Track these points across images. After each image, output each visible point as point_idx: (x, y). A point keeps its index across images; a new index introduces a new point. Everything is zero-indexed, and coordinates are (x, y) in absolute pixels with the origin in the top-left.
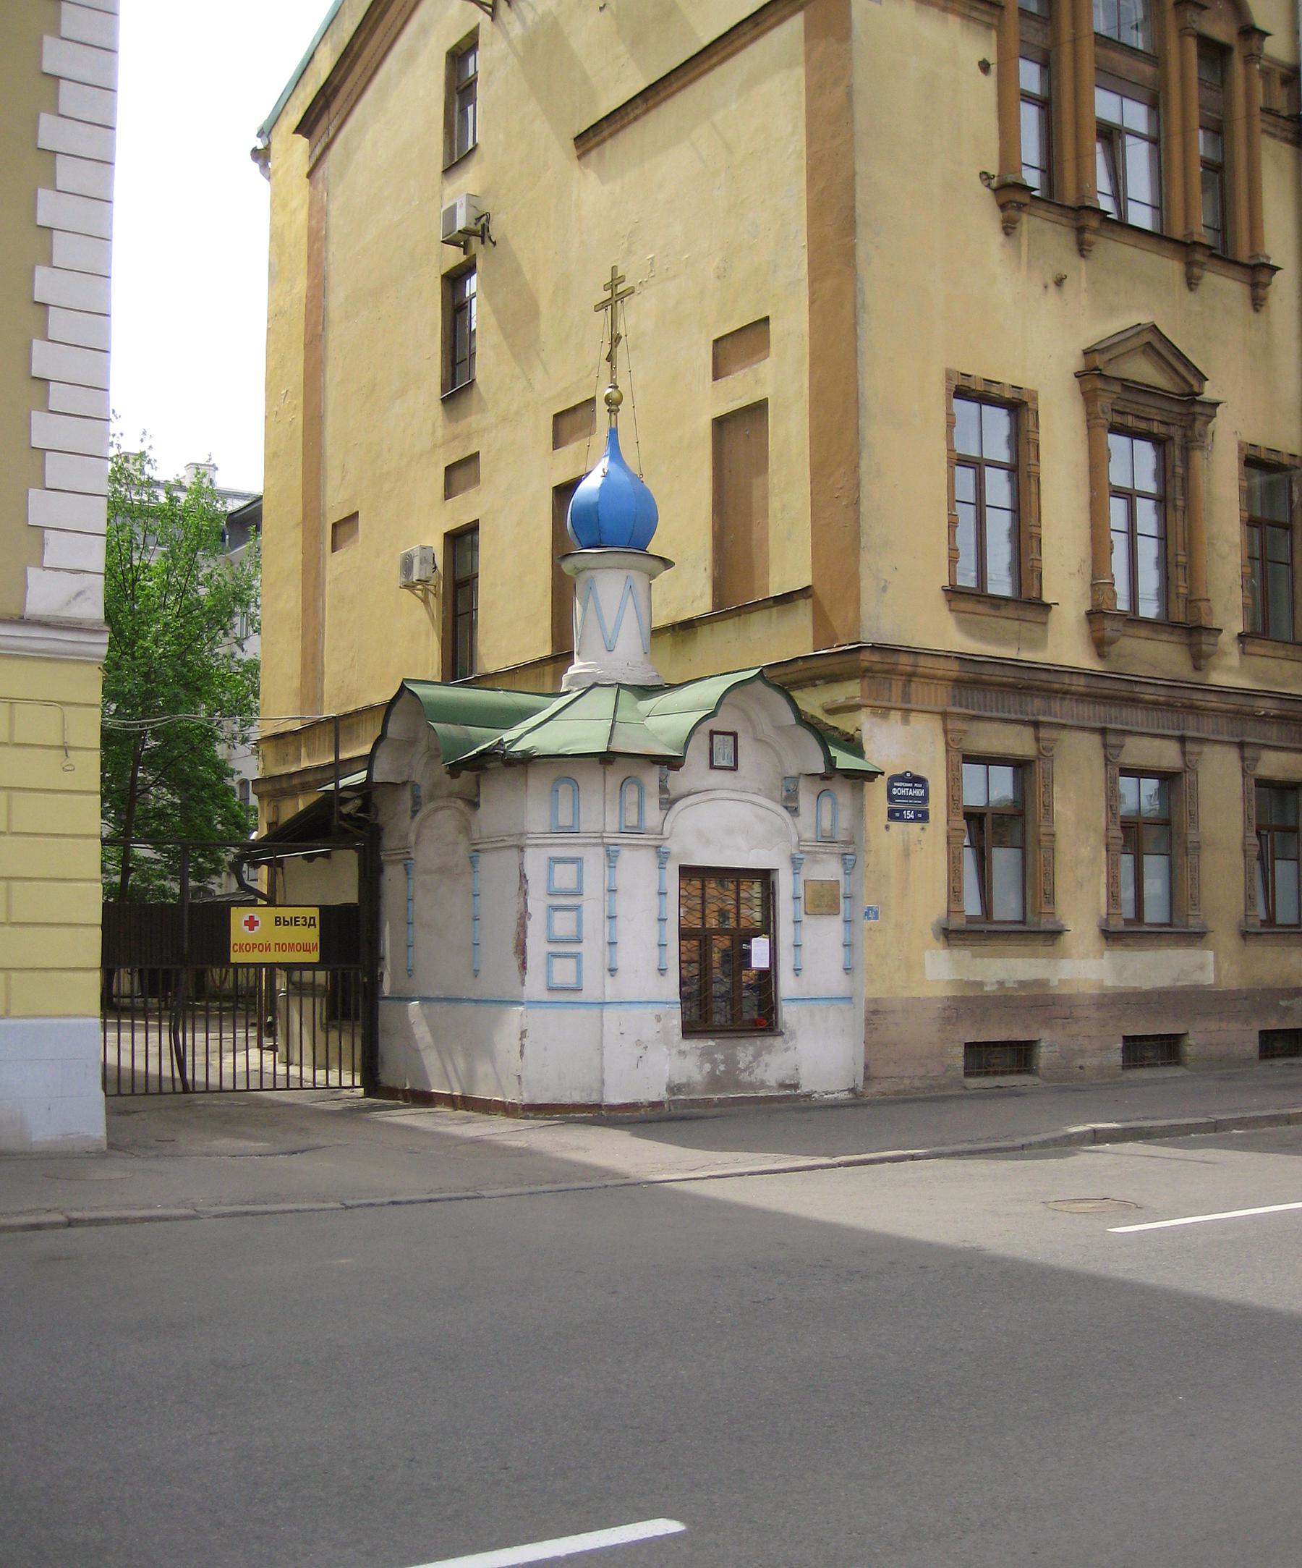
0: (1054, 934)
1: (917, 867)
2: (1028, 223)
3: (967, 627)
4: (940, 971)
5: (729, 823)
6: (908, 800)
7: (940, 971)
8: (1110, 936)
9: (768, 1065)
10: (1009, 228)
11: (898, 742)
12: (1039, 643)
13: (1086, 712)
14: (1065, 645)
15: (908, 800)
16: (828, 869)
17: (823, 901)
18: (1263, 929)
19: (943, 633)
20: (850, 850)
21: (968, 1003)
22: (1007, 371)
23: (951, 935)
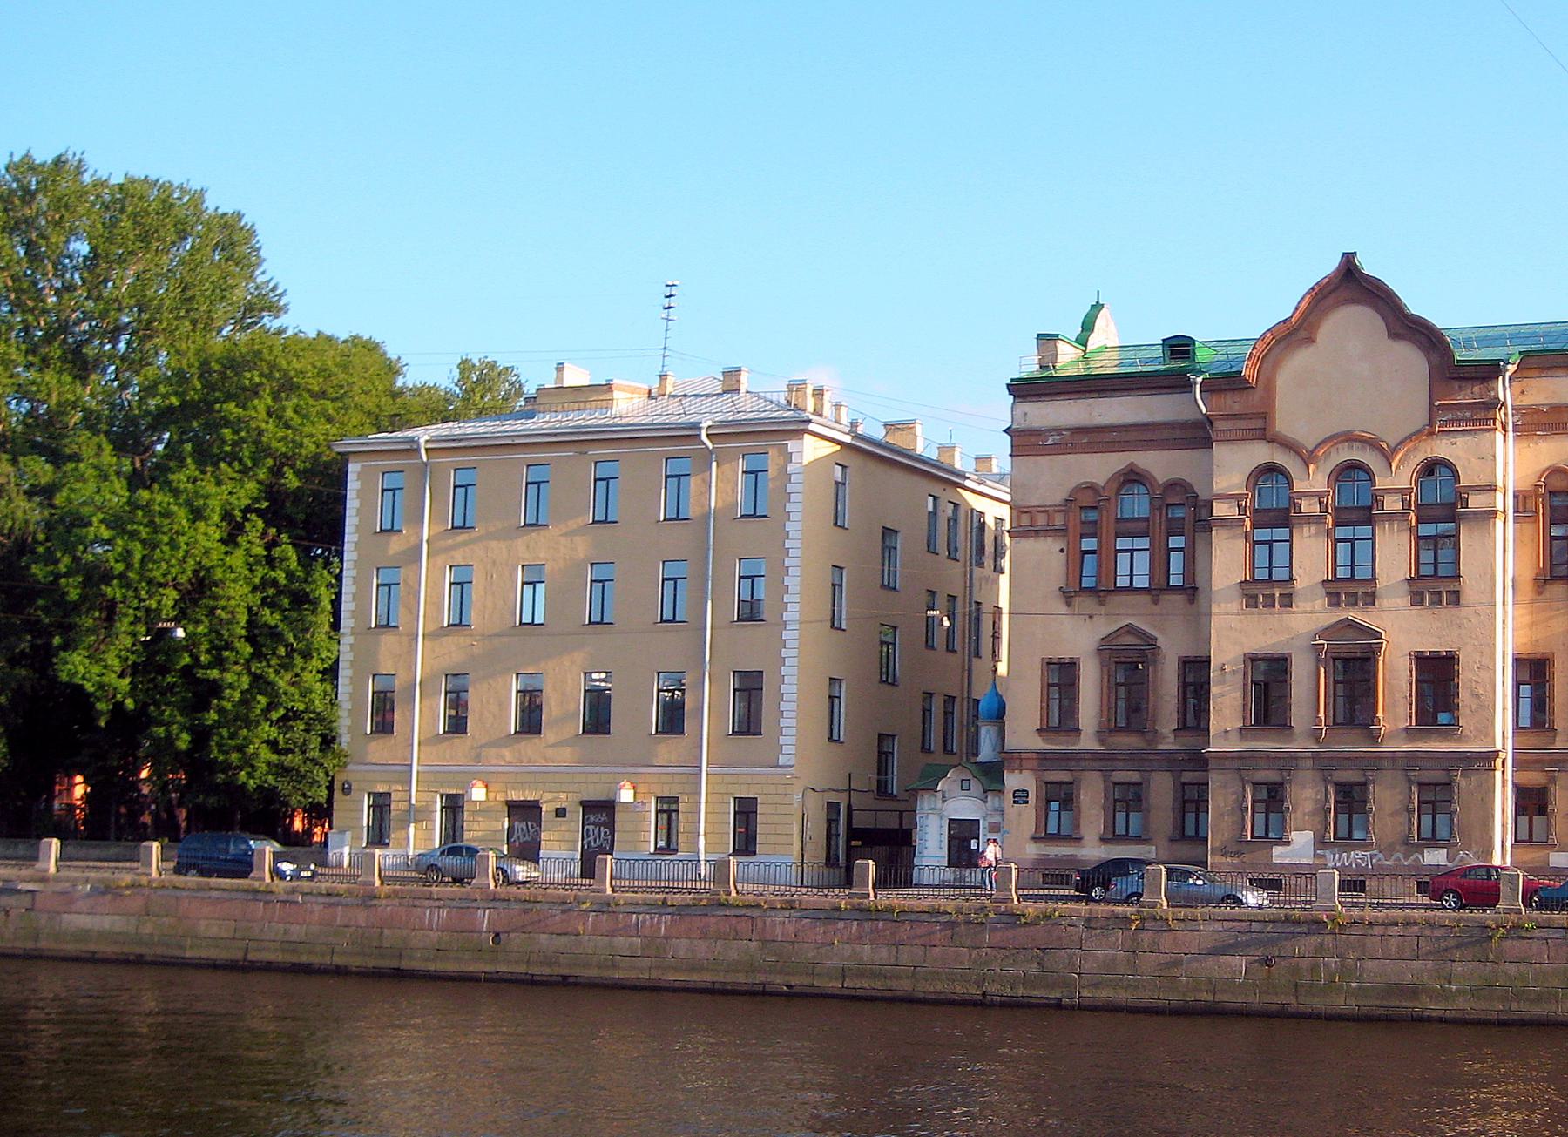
1: (1024, 818)
2: (1077, 600)
3: (1046, 741)
4: (1032, 851)
5: (965, 806)
6: (1020, 797)
7: (1032, 851)
8: (1103, 840)
10: (1069, 604)
12: (1077, 742)
13: (1096, 765)
14: (1087, 742)
15: (1020, 797)
17: (995, 828)
18: (1111, 837)
19: (1039, 744)
21: (1042, 862)
22: (1065, 654)
23: (1035, 839)
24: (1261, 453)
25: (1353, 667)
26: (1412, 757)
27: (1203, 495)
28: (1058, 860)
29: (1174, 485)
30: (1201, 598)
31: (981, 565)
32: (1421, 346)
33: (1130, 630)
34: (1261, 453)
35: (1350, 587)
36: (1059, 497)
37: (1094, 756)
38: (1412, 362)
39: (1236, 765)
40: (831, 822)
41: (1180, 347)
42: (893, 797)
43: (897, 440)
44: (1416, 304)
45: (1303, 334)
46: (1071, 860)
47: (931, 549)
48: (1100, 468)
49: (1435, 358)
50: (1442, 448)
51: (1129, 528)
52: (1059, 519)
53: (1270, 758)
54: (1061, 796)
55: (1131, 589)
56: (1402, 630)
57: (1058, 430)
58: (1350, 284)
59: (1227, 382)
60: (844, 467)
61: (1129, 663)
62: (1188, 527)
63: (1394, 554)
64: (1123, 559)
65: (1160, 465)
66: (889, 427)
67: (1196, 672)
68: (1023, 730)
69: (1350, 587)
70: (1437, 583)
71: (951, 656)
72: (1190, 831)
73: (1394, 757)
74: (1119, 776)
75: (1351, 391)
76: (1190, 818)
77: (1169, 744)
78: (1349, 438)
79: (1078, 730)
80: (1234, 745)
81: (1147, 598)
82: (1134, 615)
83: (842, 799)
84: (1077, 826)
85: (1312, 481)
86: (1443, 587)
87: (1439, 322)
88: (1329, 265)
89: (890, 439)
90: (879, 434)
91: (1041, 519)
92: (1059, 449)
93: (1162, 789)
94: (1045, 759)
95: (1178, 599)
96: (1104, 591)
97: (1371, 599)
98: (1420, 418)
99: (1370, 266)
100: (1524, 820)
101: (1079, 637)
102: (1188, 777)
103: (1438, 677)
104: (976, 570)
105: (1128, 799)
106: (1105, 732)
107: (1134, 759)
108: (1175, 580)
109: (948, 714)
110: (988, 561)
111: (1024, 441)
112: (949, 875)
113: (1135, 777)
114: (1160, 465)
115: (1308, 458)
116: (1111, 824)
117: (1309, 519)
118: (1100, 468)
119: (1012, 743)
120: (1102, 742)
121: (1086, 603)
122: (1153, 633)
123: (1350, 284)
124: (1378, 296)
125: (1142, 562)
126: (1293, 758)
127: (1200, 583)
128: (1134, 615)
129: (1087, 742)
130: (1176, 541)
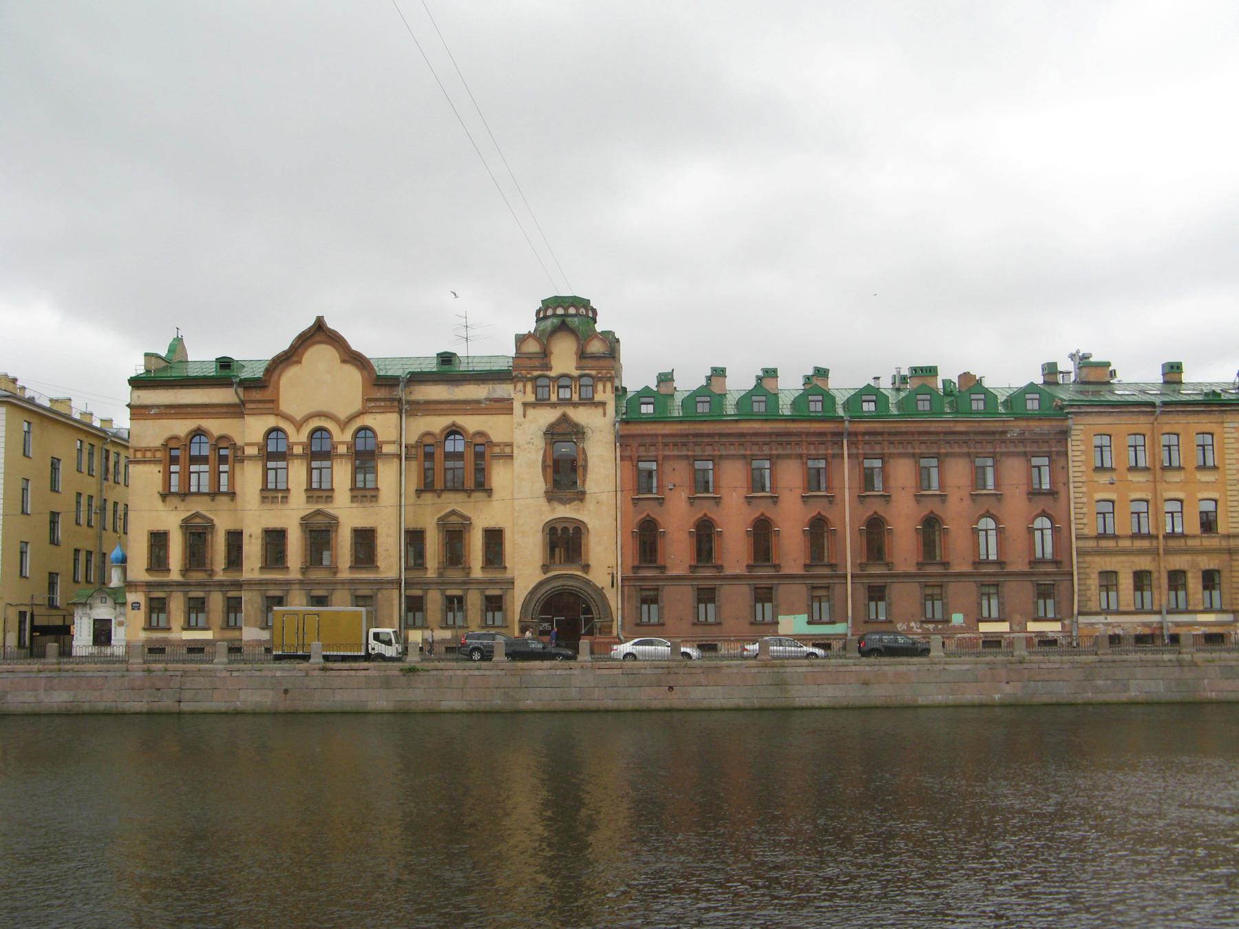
0: (169, 629)
1: (139, 617)
4: (143, 635)
5: (103, 611)
6: (136, 606)
7: (143, 635)
9: (108, 651)
11: (131, 597)
13: (181, 588)
15: (136, 606)
16: (122, 619)
17: (121, 624)
19: (146, 577)
20: (124, 614)
21: (149, 641)
22: (160, 527)
23: (145, 629)
24: (271, 421)
25: (319, 535)
26: (352, 582)
27: (239, 443)
28: (157, 640)
29: (222, 438)
30: (239, 498)
31: (106, 479)
32: (358, 367)
33: (197, 515)
34: (271, 421)
35: (319, 492)
36: (158, 443)
37: (179, 584)
38: (353, 376)
39: (258, 587)
40: (22, 622)
41: (225, 363)
42: (57, 608)
43: (61, 409)
44: (355, 346)
45: (295, 359)
46: (166, 641)
47: (79, 471)
48: (181, 427)
49: (366, 373)
50: (368, 420)
51: (202, 460)
52: (159, 455)
53: (275, 583)
54: (157, 606)
55: (199, 493)
56: (349, 516)
57: (158, 407)
58: (319, 332)
59: (250, 385)
60: (29, 423)
61: (197, 535)
62: (231, 459)
63: (341, 474)
64: (194, 477)
65: (216, 426)
66: (51, 400)
67: (235, 539)
68: (138, 569)
69: (319, 492)
70: (364, 493)
71: (90, 530)
72: (232, 623)
73: (343, 582)
74: (192, 595)
75: (321, 390)
76: (232, 616)
77: (220, 576)
78: (319, 415)
79: (169, 570)
80: (256, 575)
81: (208, 498)
82: (200, 506)
83: (28, 610)
84: (168, 621)
85: (298, 437)
86: (368, 494)
87: (368, 353)
88: (308, 323)
89: (55, 408)
90: (48, 404)
91: (139, 455)
92: (159, 416)
93: (216, 601)
94: (149, 585)
95: (225, 499)
96: (185, 495)
97: (329, 499)
98: (357, 405)
99: (331, 324)
100: (410, 615)
101: (171, 520)
102: (231, 594)
103: (365, 539)
104: (105, 483)
105: (197, 606)
106: (185, 571)
107: (200, 585)
108: (223, 489)
109: (88, 561)
110: (111, 477)
111: (137, 411)
112: (95, 650)
113: (201, 594)
114: (216, 426)
115: (298, 426)
116: (188, 621)
117: (297, 456)
118: (181, 427)
119: (131, 576)
120: (183, 576)
121: (175, 501)
122: (211, 517)
123: (319, 332)
124: (336, 340)
125: (205, 478)
126: (288, 583)
127: (238, 489)
128: (200, 506)
129: (175, 575)
130: (223, 468)
